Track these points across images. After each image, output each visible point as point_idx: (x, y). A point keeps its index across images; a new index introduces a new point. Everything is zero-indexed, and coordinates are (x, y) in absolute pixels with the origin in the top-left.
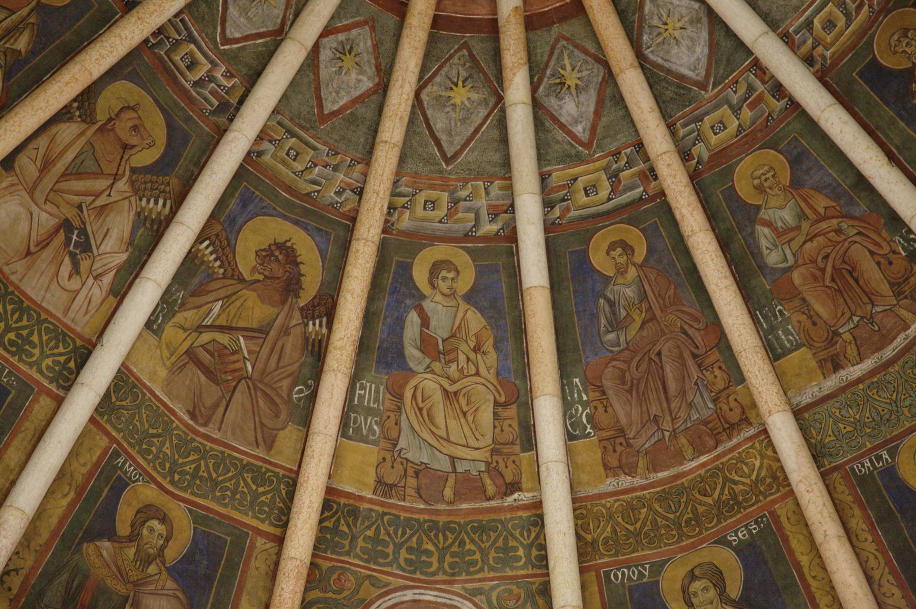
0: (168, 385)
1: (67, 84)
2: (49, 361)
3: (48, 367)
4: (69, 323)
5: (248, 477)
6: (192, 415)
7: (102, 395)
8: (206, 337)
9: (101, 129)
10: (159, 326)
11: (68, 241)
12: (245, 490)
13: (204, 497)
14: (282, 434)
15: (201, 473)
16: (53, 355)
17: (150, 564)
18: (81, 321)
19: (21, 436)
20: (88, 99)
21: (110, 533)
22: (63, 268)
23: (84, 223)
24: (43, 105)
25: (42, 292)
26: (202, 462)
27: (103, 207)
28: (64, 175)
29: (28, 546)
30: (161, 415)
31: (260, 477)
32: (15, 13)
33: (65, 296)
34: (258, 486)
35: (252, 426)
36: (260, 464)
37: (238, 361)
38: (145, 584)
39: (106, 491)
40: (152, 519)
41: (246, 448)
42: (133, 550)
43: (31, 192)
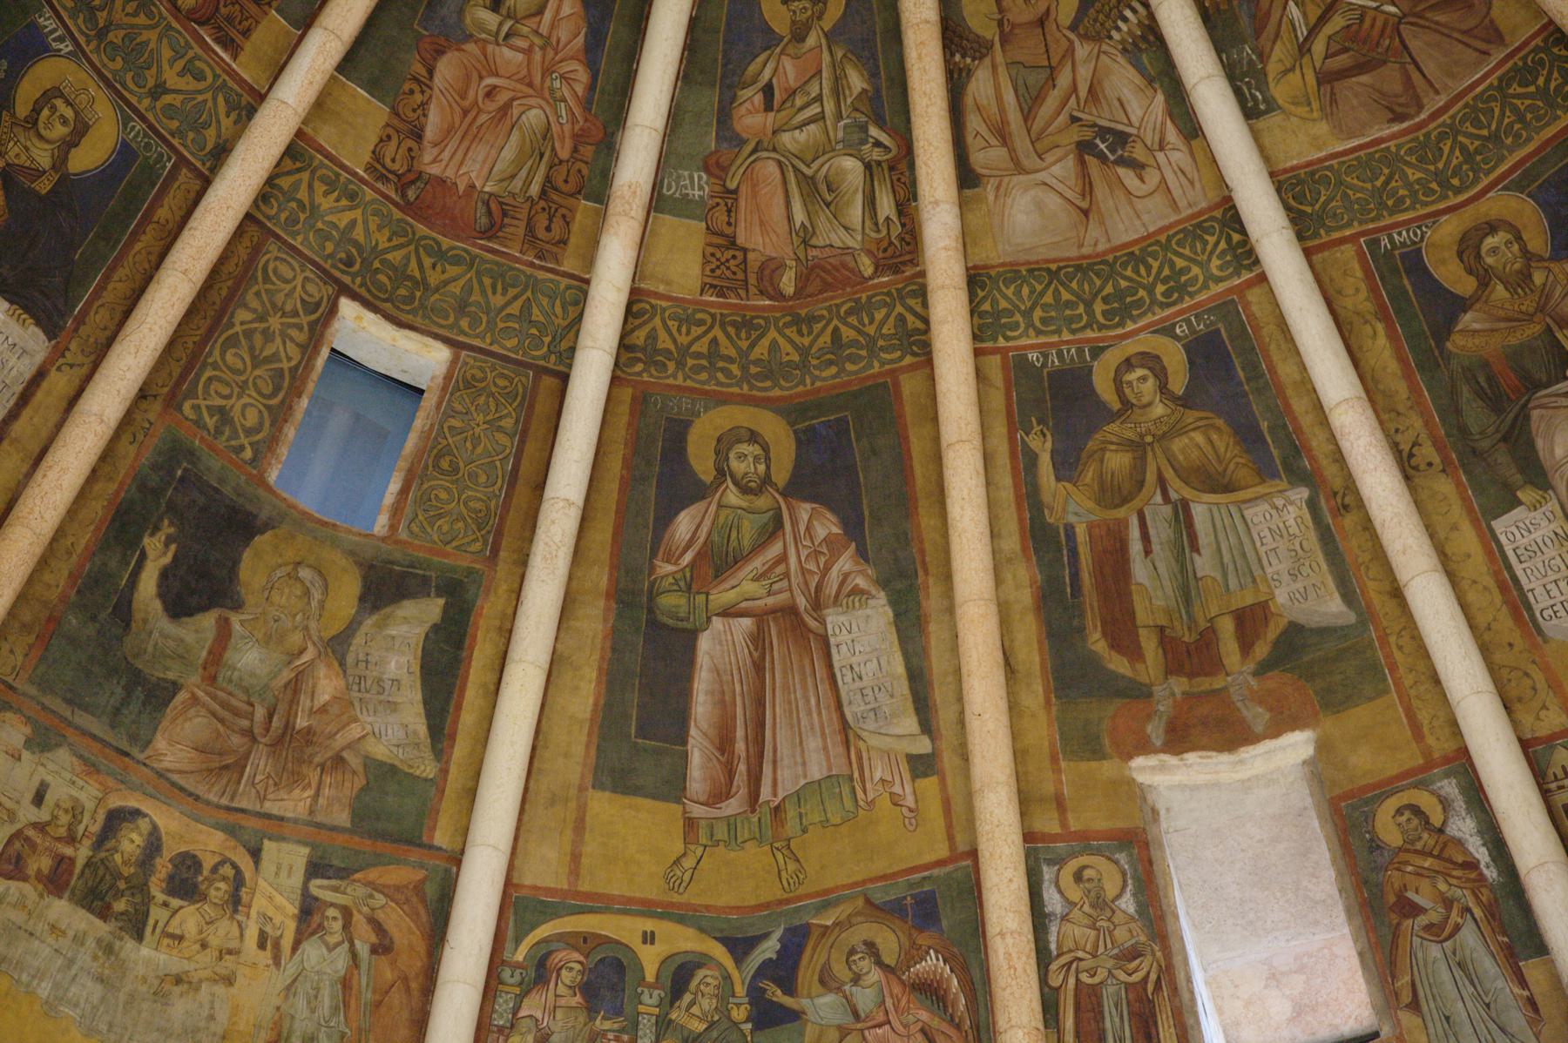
0: (1341, 131)
1: (920, 57)
2: (1215, 262)
3: (1221, 268)
4: (1190, 212)
5: (1515, 89)
6: (1399, 118)
7: (1286, 223)
8: (1319, 47)
9: (1004, 40)
10: (1264, 100)
11: (1102, 158)
12: (1528, 102)
13: (1502, 159)
14: (1495, 13)
15: (1471, 148)
16: (1211, 253)
17: (1530, 276)
18: (1194, 199)
19: (1273, 347)
20: (961, 37)
21: (1461, 305)
22: (1127, 182)
23: (1095, 125)
24: (925, 101)
25: (1138, 223)
26: (1460, 138)
27: (1091, 90)
28: (1026, 120)
29: (1399, 414)
30: (1370, 160)
31: (1524, 74)
32: (820, 72)
33: (1159, 199)
34: (1534, 82)
35: (1460, 46)
36: (1510, 64)
37: (1374, 19)
38: (1548, 297)
39: (1406, 282)
40: (1481, 242)
41: (1481, 73)
42: (1500, 287)
43: (1020, 169)
